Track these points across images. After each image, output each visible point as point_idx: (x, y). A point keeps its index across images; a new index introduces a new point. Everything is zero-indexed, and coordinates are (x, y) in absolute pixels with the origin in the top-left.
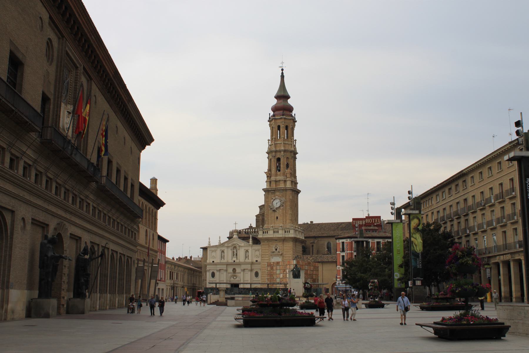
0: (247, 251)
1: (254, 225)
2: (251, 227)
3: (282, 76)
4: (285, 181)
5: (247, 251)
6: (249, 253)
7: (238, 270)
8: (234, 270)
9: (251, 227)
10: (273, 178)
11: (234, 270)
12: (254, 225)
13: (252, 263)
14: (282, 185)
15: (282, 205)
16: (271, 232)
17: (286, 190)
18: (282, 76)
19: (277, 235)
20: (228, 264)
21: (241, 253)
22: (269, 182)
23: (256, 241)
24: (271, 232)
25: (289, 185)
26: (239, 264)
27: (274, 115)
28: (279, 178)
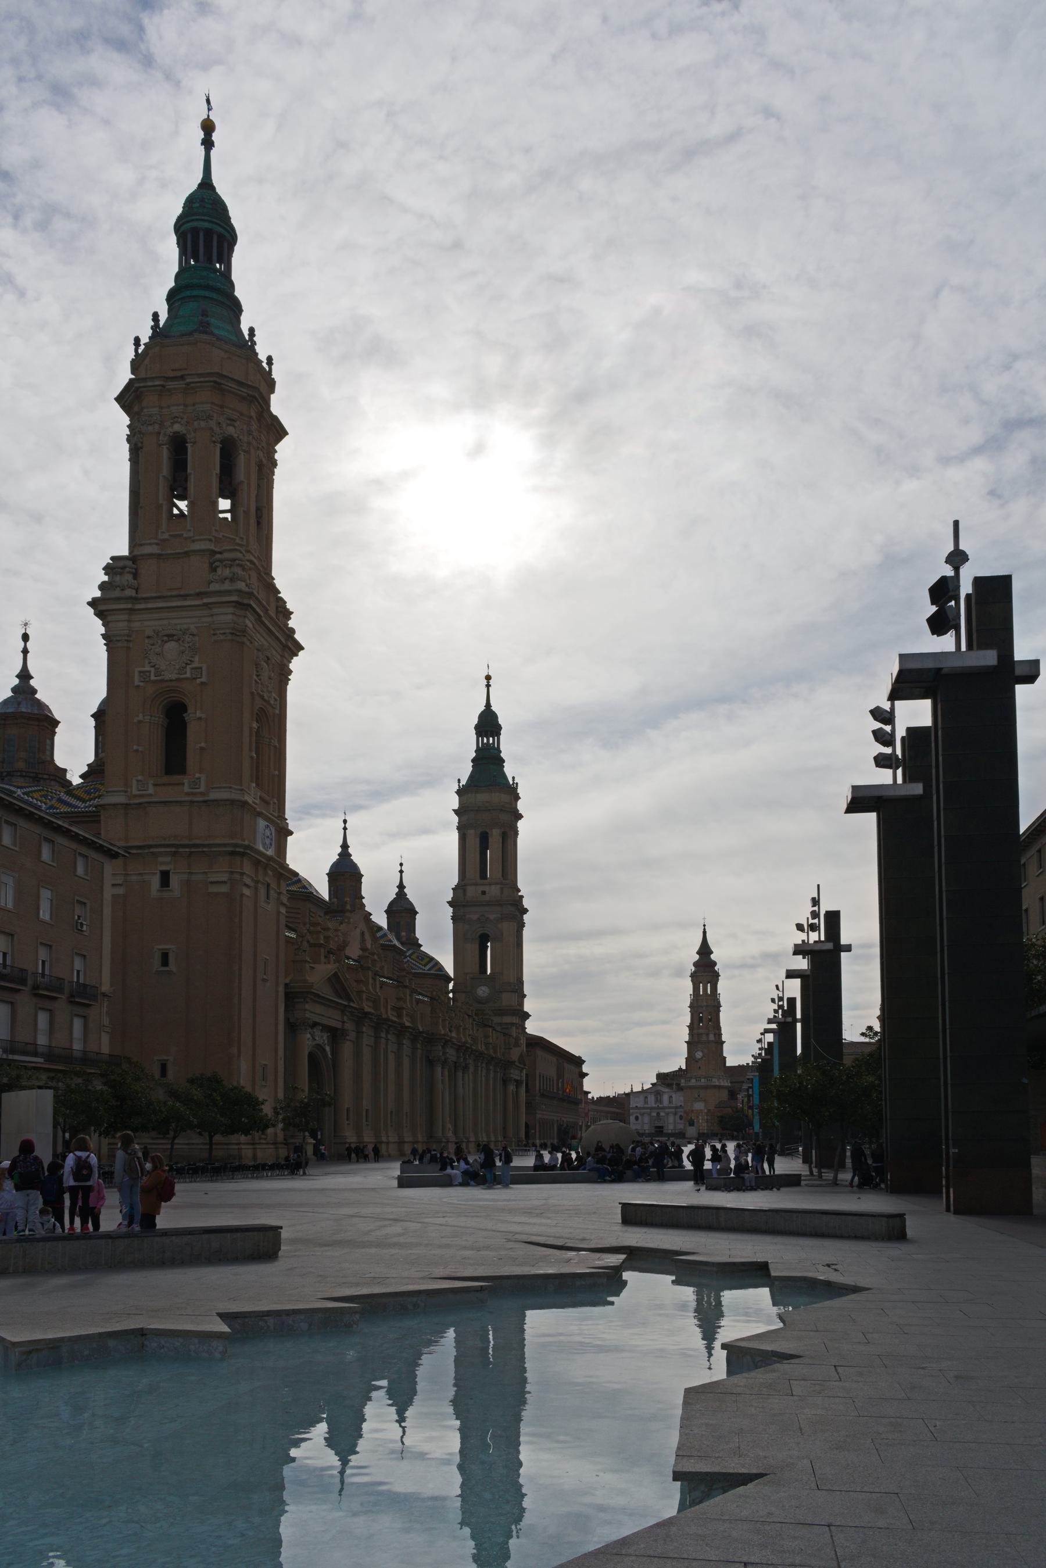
0: (671, 1097)
1: (684, 1067)
2: (680, 1069)
3: (705, 933)
4: (708, 1034)
5: (671, 1097)
6: (673, 1098)
7: (662, 1114)
8: (658, 1114)
9: (680, 1069)
10: (695, 1031)
11: (658, 1114)
12: (684, 1067)
13: (676, 1108)
14: (704, 1038)
15: (704, 1056)
16: (693, 1081)
17: (709, 1042)
18: (705, 933)
19: (698, 1084)
20: (651, 1108)
21: (665, 1098)
22: (691, 1034)
23: (680, 1088)
24: (693, 1081)
25: (711, 1037)
26: (664, 1108)
27: (695, 972)
28: (701, 1031)
